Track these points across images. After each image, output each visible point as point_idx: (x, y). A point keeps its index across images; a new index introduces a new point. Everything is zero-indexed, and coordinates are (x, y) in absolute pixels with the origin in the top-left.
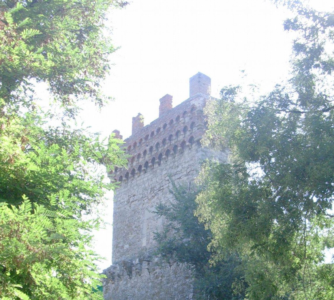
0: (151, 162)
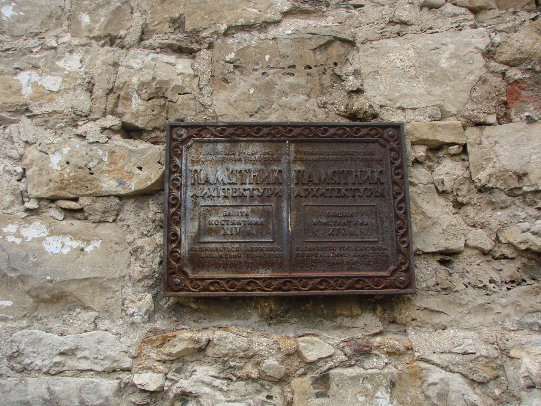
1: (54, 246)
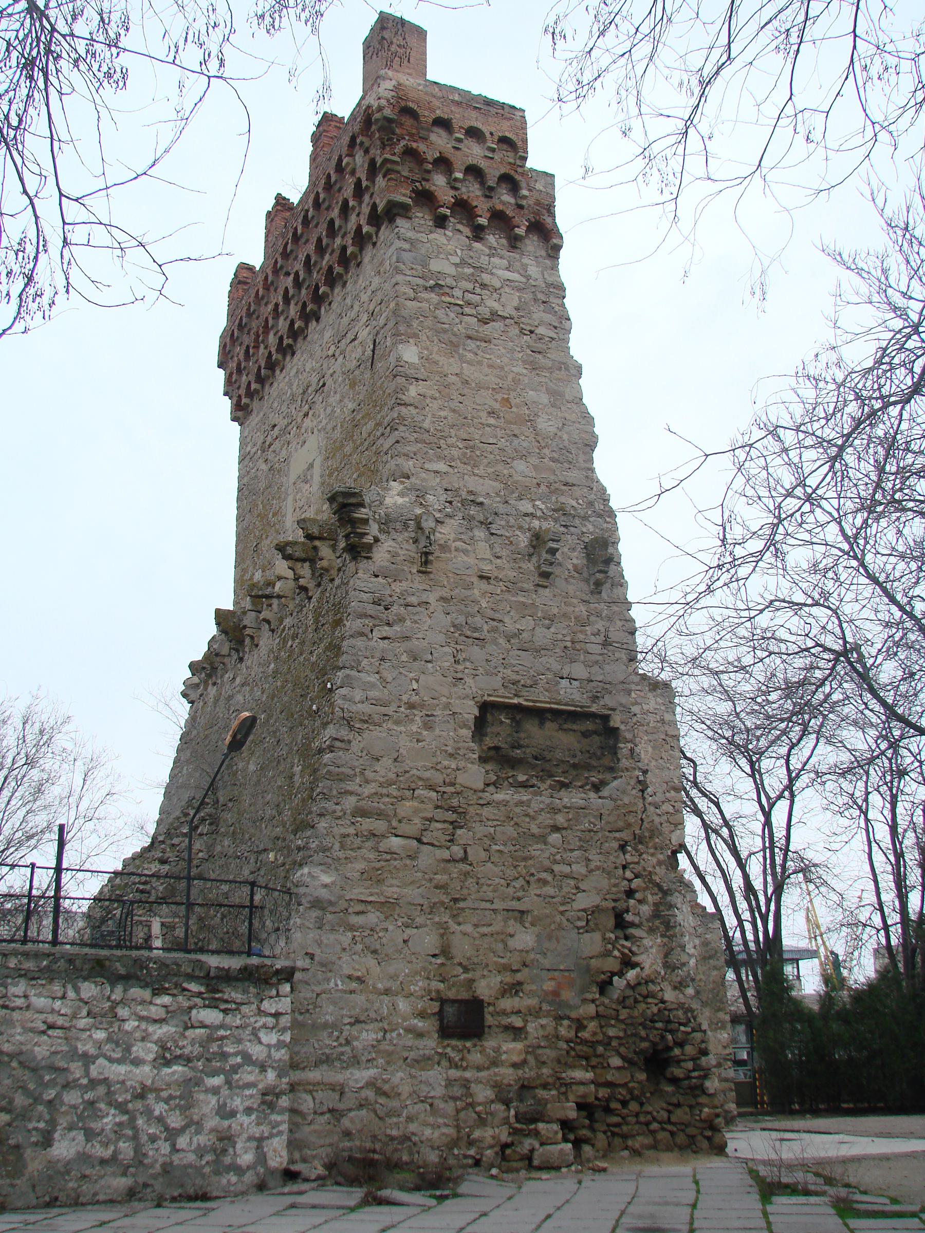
0: (300, 318)
1: (420, 1024)
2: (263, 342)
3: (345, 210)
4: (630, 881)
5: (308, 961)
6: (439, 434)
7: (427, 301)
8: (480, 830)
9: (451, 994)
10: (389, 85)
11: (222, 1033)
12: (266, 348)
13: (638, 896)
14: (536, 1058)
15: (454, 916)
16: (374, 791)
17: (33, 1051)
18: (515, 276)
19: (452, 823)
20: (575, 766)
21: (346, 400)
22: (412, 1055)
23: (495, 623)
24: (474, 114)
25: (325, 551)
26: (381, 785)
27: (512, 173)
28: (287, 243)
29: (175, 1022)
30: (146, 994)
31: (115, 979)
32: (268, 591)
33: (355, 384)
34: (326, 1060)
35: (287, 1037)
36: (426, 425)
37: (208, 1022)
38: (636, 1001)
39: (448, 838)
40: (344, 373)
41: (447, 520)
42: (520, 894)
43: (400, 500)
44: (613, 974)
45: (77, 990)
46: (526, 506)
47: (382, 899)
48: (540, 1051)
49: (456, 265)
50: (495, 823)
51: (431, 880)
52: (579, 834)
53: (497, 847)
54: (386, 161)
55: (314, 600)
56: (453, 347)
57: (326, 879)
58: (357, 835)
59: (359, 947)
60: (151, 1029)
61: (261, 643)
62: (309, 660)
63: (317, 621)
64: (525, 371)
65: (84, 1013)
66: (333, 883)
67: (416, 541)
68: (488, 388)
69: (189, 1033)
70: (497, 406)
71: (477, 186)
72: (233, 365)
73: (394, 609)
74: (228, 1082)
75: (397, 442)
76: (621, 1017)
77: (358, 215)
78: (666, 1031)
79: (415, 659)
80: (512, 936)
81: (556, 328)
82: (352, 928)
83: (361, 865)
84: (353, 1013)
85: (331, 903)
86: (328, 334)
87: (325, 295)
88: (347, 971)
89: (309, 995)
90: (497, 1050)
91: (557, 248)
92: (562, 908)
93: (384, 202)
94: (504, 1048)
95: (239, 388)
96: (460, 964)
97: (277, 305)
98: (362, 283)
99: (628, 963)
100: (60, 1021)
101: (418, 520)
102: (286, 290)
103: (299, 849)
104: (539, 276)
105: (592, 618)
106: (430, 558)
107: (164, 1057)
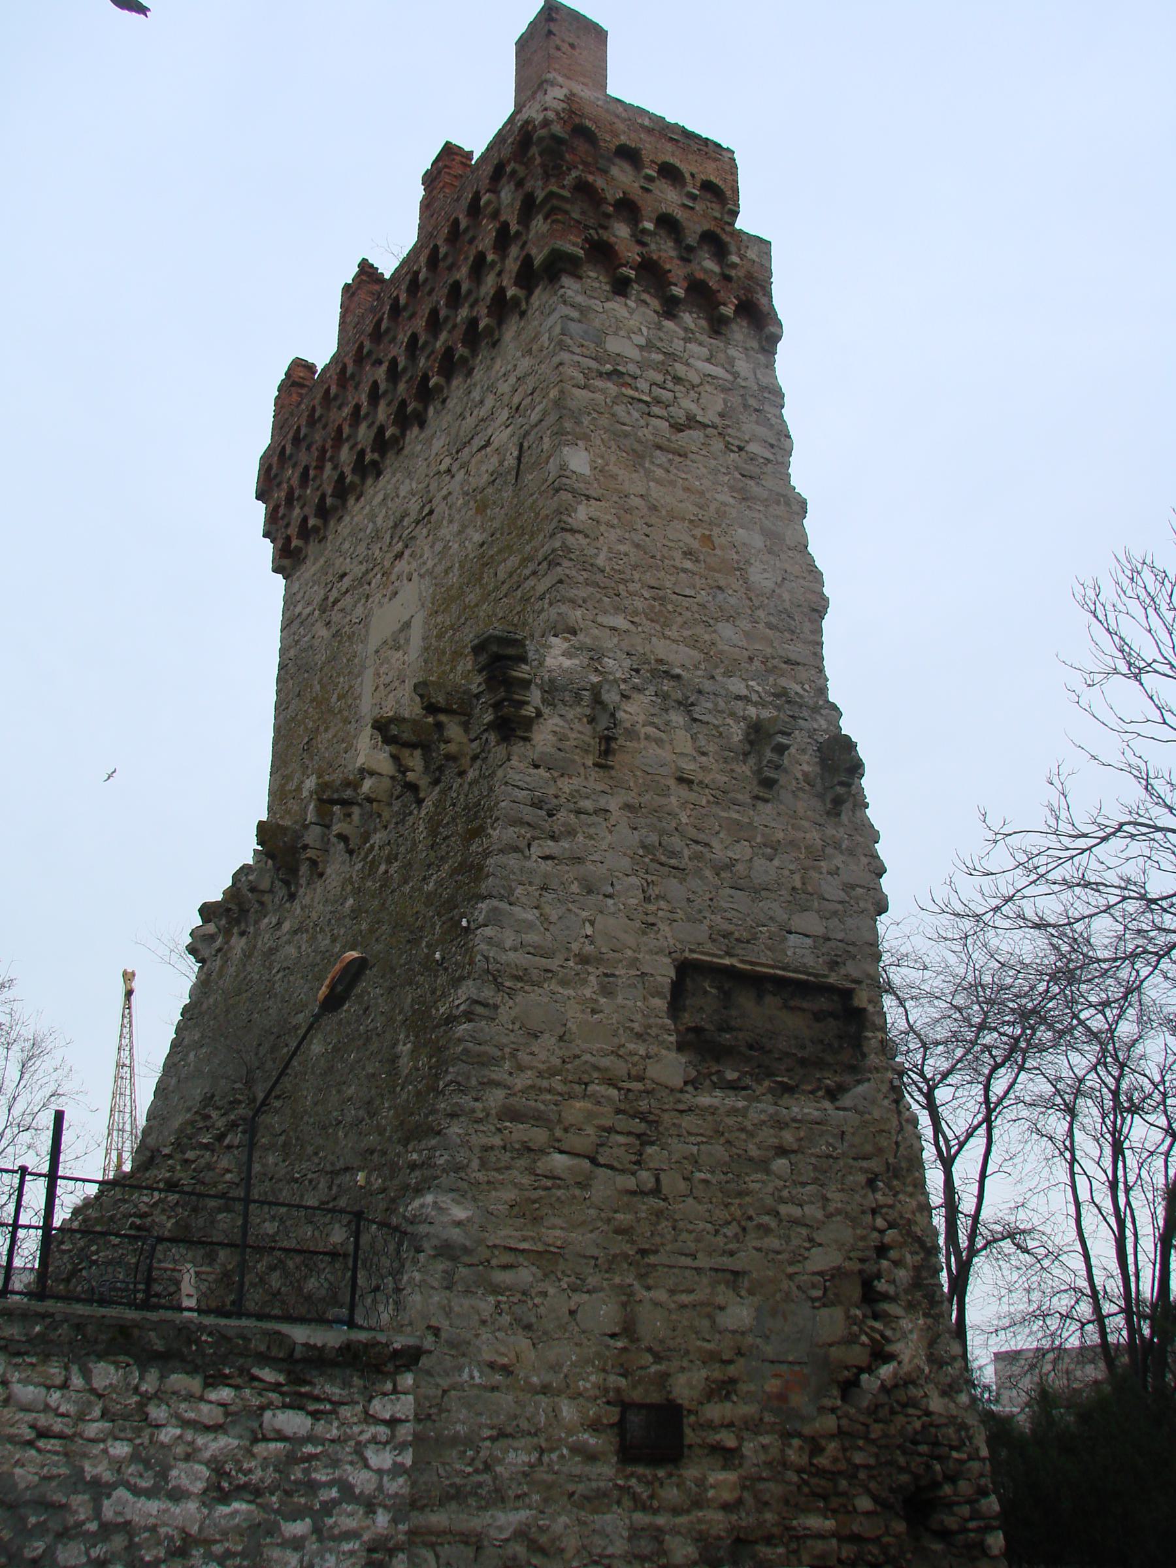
0: (394, 424)
1: (592, 1441)
2: (331, 459)
3: (479, 266)
4: (882, 1232)
5: (431, 1338)
6: (617, 576)
7: (603, 391)
8: (679, 1148)
9: (637, 1395)
10: (559, 93)
11: (309, 1449)
12: (335, 468)
13: (893, 1254)
14: (755, 1497)
15: (641, 1277)
16: (529, 1082)
17: (12, 1474)
18: (718, 371)
19: (639, 1136)
20: (803, 1062)
21: (470, 531)
22: (581, 1488)
23: (699, 848)
24: (669, 147)
25: (454, 730)
26: (540, 1075)
27: (719, 231)
28: (380, 320)
29: (238, 1430)
30: (195, 1384)
31: (146, 1358)
32: (348, 794)
33: (486, 507)
34: (456, 1496)
35: (407, 1459)
36: (600, 561)
37: (289, 1431)
38: (893, 1412)
39: (634, 1158)
40: (466, 494)
41: (635, 695)
42: (733, 1246)
43: (567, 663)
44: (861, 1370)
45: (86, 1374)
46: (737, 686)
47: (540, 1247)
48: (761, 1486)
49: (641, 347)
50: (700, 1139)
51: (609, 1221)
52: (813, 1160)
53: (702, 1175)
54: (551, 195)
55: (428, 803)
56: (637, 458)
57: (460, 1213)
58: (504, 1148)
59: (506, 1319)
60: (200, 1441)
61: (329, 871)
62: (420, 889)
63: (433, 832)
64: (732, 501)
65: (97, 1412)
66: (469, 1219)
67: (592, 720)
68: (683, 519)
69: (259, 1448)
70: (695, 545)
71: (671, 244)
72: (280, 495)
73: (562, 815)
74: (317, 1530)
75: (561, 582)
76: (873, 1436)
77: (499, 274)
78: (933, 1457)
79: (590, 892)
80: (722, 1308)
81: (772, 446)
82: (496, 1290)
83: (509, 1195)
84: (495, 1421)
85: (466, 1250)
86: (437, 444)
87: (439, 388)
88: (487, 1356)
89: (432, 1392)
90: (701, 1482)
91: (775, 339)
92: (790, 1270)
93: (546, 251)
94: (711, 1480)
95: (287, 526)
96: (649, 1350)
97: (357, 407)
98: (499, 367)
99: (880, 1355)
100: (58, 1426)
101: (596, 691)
102: (375, 385)
103: (413, 1166)
104: (751, 376)
105: (829, 850)
106: (613, 745)
107: (220, 1488)
